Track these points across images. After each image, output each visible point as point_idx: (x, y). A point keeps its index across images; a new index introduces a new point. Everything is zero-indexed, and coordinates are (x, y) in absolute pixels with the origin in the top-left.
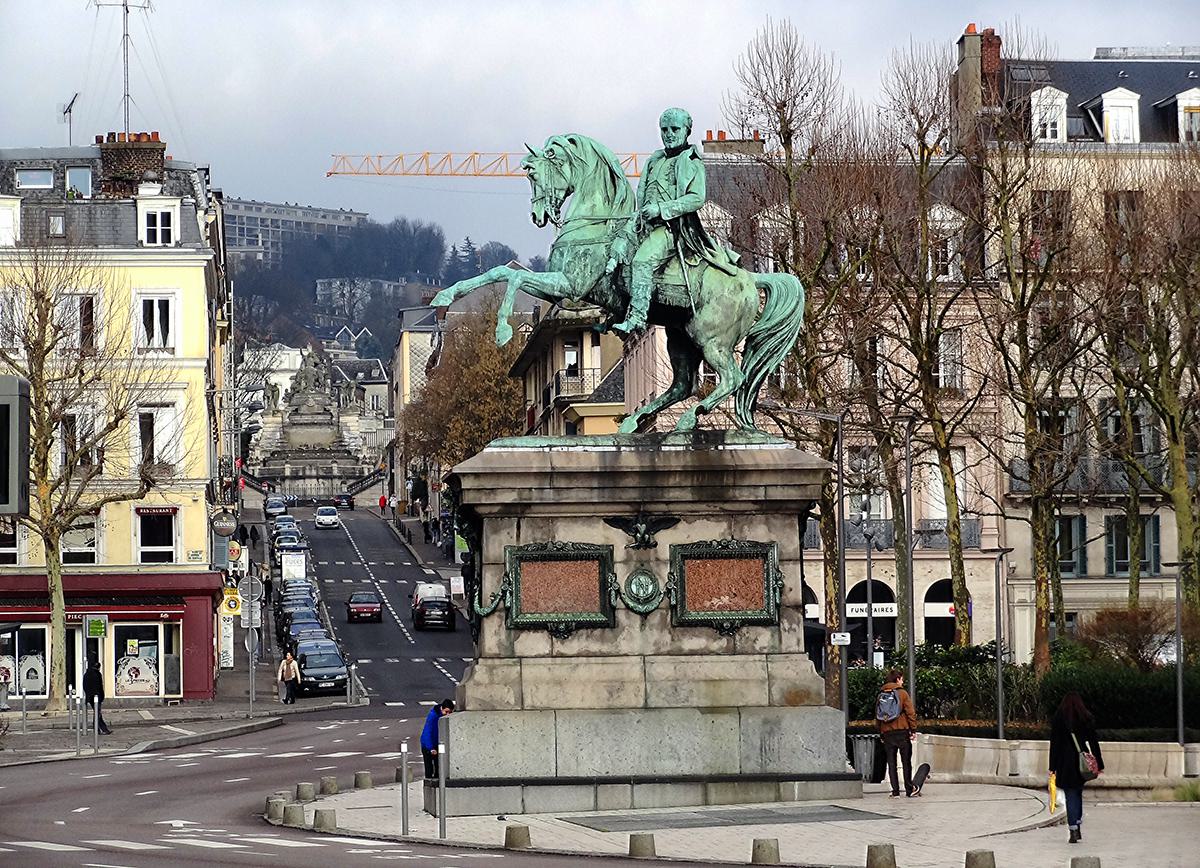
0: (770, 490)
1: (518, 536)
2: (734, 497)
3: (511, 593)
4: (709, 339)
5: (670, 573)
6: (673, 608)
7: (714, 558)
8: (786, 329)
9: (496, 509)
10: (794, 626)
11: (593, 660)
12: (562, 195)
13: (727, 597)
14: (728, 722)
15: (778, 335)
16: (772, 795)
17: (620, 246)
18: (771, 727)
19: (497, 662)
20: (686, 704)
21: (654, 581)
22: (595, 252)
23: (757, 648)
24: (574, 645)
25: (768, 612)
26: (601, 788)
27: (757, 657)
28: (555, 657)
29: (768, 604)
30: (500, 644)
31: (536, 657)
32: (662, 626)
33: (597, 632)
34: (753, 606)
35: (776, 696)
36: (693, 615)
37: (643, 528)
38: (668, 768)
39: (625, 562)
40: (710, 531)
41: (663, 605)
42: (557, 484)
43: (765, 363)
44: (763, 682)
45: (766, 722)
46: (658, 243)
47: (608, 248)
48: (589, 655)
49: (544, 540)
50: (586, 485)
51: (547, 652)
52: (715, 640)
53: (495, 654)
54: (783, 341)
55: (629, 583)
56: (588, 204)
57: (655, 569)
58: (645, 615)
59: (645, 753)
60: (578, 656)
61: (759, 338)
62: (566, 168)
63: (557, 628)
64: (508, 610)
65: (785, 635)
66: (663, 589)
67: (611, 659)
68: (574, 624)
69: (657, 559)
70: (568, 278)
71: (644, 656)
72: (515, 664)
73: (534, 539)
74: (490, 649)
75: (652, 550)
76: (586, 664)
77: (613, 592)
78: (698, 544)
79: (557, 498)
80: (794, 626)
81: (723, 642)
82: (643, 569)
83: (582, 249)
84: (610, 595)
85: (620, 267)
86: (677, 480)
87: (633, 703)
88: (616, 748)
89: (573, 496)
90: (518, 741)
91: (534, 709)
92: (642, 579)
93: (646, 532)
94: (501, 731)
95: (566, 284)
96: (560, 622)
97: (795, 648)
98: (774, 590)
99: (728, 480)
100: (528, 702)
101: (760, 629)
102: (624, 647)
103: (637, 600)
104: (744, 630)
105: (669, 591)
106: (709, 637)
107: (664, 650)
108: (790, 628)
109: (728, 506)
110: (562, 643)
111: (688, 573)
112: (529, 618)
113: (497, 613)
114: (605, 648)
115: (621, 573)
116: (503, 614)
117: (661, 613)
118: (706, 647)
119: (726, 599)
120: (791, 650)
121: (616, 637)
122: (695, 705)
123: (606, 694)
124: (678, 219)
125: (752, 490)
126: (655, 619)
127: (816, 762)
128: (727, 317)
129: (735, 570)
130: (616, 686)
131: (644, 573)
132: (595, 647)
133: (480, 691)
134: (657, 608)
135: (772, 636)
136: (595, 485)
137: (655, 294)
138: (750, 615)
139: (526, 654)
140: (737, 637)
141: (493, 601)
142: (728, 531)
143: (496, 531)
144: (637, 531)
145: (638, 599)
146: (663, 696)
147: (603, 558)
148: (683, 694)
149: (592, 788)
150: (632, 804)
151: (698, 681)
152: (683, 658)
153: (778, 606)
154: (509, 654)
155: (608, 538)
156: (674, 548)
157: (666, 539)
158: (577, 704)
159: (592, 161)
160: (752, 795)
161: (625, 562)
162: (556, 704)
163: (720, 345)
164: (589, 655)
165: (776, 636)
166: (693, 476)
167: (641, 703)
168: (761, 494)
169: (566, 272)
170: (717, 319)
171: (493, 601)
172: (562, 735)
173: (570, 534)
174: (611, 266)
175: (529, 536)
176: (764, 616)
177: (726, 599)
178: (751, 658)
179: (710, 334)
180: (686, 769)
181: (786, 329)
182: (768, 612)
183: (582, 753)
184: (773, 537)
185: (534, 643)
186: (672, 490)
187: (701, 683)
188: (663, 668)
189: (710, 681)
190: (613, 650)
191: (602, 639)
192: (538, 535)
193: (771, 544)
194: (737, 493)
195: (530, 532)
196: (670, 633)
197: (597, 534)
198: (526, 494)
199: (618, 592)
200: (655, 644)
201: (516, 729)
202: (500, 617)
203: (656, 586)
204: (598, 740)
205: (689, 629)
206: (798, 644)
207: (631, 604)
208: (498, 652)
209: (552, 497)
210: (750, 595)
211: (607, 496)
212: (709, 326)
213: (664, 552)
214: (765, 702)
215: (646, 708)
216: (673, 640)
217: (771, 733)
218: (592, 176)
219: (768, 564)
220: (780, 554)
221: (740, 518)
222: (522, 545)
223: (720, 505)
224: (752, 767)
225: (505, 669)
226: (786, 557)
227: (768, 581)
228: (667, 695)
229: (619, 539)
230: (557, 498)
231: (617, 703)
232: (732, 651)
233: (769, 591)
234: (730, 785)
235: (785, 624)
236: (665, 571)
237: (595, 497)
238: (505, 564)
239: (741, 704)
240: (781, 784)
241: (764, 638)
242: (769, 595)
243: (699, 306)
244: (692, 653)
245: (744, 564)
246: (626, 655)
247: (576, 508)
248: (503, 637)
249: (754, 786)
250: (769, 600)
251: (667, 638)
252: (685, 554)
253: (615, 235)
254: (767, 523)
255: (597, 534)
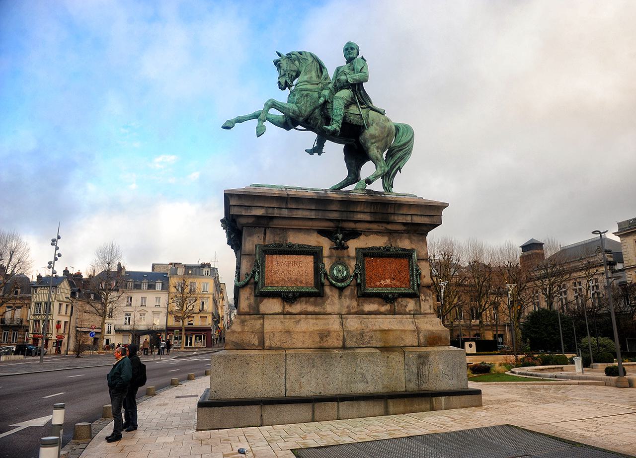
0: (414, 217)
1: (264, 239)
2: (395, 220)
3: (259, 273)
4: (372, 143)
5: (356, 264)
6: (358, 285)
7: (382, 257)
8: (407, 148)
9: (251, 221)
10: (427, 298)
11: (309, 316)
12: (294, 74)
13: (389, 280)
14: (396, 357)
15: (404, 150)
16: (428, 406)
17: (326, 92)
18: (423, 359)
19: (248, 317)
20: (369, 345)
21: (347, 269)
22: (312, 95)
23: (407, 310)
24: (297, 308)
25: (414, 289)
26: (317, 405)
27: (408, 316)
28: (285, 314)
29: (413, 284)
30: (250, 306)
31: (273, 314)
32: (352, 297)
33: (312, 299)
34: (404, 286)
35: (422, 340)
36: (370, 290)
37: (340, 236)
38: (360, 388)
39: (329, 257)
40: (378, 242)
41: (352, 284)
42: (290, 206)
43: (397, 164)
44: (414, 331)
45: (420, 357)
46: (345, 93)
47: (319, 93)
48: (307, 313)
49: (280, 242)
50: (308, 207)
51: (281, 311)
52: (383, 305)
53: (246, 312)
54: (406, 154)
55: (332, 269)
56: (308, 76)
57: (347, 262)
58: (341, 289)
59: (345, 379)
60: (300, 314)
61: (394, 151)
62: (297, 62)
63: (287, 296)
64: (256, 283)
65: (422, 303)
66: (351, 273)
67: (321, 316)
68: (298, 294)
69: (349, 256)
70: (297, 106)
71: (342, 314)
72: (259, 318)
73: (274, 241)
74: (243, 309)
75: (345, 251)
76: (306, 319)
77: (323, 274)
78: (373, 248)
79: (290, 214)
80: (427, 298)
81: (387, 307)
82: (340, 261)
83: (305, 93)
84: (321, 276)
85: (326, 102)
86: (362, 208)
87: (336, 345)
88: (326, 376)
89: (300, 214)
90: (260, 371)
91: (271, 348)
92: (340, 267)
93: (343, 239)
94: (248, 364)
95: (296, 109)
96: (289, 292)
97: (429, 311)
98: (417, 276)
99: (391, 210)
100: (267, 344)
101: (409, 300)
102: (329, 309)
103: (337, 279)
104: (400, 300)
105: (356, 275)
106: (379, 304)
107: (353, 311)
108: (425, 300)
109: (390, 227)
110: (290, 306)
111: (366, 265)
112: (269, 289)
113: (249, 286)
114: (317, 309)
115: (327, 264)
116: (253, 286)
117: (351, 289)
118: (378, 310)
119: (388, 281)
120: (426, 312)
121: (324, 303)
122: (374, 345)
123: (318, 339)
124: (355, 84)
125: (404, 217)
126: (347, 292)
127: (450, 382)
128: (382, 133)
129: (392, 265)
130: (324, 335)
131: (340, 264)
132: (310, 309)
133: (234, 336)
134: (349, 285)
135: (416, 304)
136: (314, 208)
137: (345, 118)
138: (403, 290)
139: (267, 313)
140: (396, 304)
141: (246, 277)
142: (388, 242)
143: (250, 235)
144: (337, 238)
145: (338, 280)
146: (355, 340)
147: (316, 253)
148: (367, 339)
149: (310, 406)
150: (338, 416)
151: (376, 331)
152: (365, 316)
153: (418, 285)
154: (255, 312)
155: (319, 242)
156: (358, 250)
157: (353, 245)
158: (300, 345)
159: (310, 59)
160: (416, 407)
161: (329, 257)
162: (285, 345)
163: (377, 148)
164: (307, 313)
165: (418, 304)
166: (371, 205)
167: (341, 344)
168: (409, 219)
169: (297, 103)
170: (377, 133)
171: (246, 277)
172: (291, 367)
173: (296, 239)
174: (322, 100)
175: (271, 239)
176: (411, 291)
177: (388, 281)
178: (405, 316)
179: (373, 141)
180: (371, 389)
181: (407, 148)
182: (414, 289)
183: (303, 380)
184: (414, 247)
185: (272, 306)
186: (359, 214)
187: (378, 332)
188: (353, 323)
189: (383, 331)
190: (322, 311)
191: (315, 304)
192: (277, 239)
193: (413, 250)
194: (396, 218)
195: (272, 236)
196: (356, 301)
197: (313, 240)
198: (270, 211)
199: (325, 274)
200: (347, 307)
201: (259, 363)
202: (250, 288)
203: (348, 272)
204: (314, 370)
205: (368, 298)
206: (430, 309)
207: (334, 282)
208: (248, 311)
209: (286, 213)
210: (402, 279)
211: (320, 215)
212: (373, 137)
213: (352, 252)
214: (416, 344)
215: (344, 347)
216: (358, 305)
217: (423, 364)
218: (311, 64)
219: (412, 262)
220: (418, 256)
221: (395, 235)
222: (266, 244)
223: (385, 225)
224: (412, 387)
225: (253, 321)
226: (421, 258)
227: (413, 271)
228: (357, 339)
229: (326, 244)
230: (290, 214)
231: (325, 345)
232: (393, 312)
233: (413, 277)
234: (403, 400)
235: (422, 297)
236: (353, 263)
237: (312, 215)
238: (255, 255)
239: (402, 345)
240: (434, 399)
241: (411, 305)
242: (413, 279)
243: (368, 125)
244: (370, 313)
245: (398, 261)
246: (330, 314)
247: (301, 223)
248: (252, 301)
249: (416, 400)
250: (413, 282)
251: (355, 304)
252: (365, 254)
253: (323, 89)
254: (410, 238)
255: (313, 240)
